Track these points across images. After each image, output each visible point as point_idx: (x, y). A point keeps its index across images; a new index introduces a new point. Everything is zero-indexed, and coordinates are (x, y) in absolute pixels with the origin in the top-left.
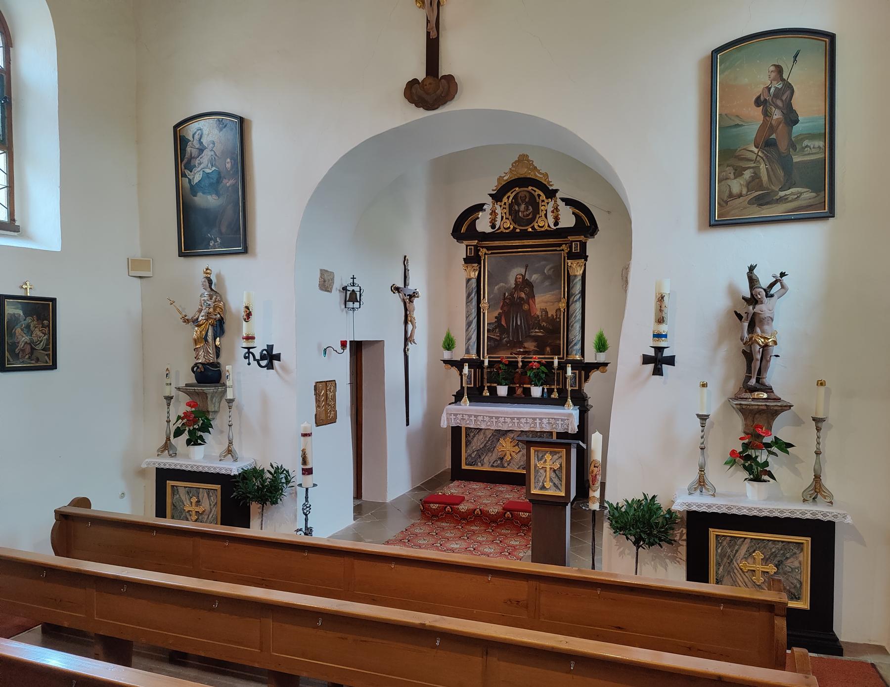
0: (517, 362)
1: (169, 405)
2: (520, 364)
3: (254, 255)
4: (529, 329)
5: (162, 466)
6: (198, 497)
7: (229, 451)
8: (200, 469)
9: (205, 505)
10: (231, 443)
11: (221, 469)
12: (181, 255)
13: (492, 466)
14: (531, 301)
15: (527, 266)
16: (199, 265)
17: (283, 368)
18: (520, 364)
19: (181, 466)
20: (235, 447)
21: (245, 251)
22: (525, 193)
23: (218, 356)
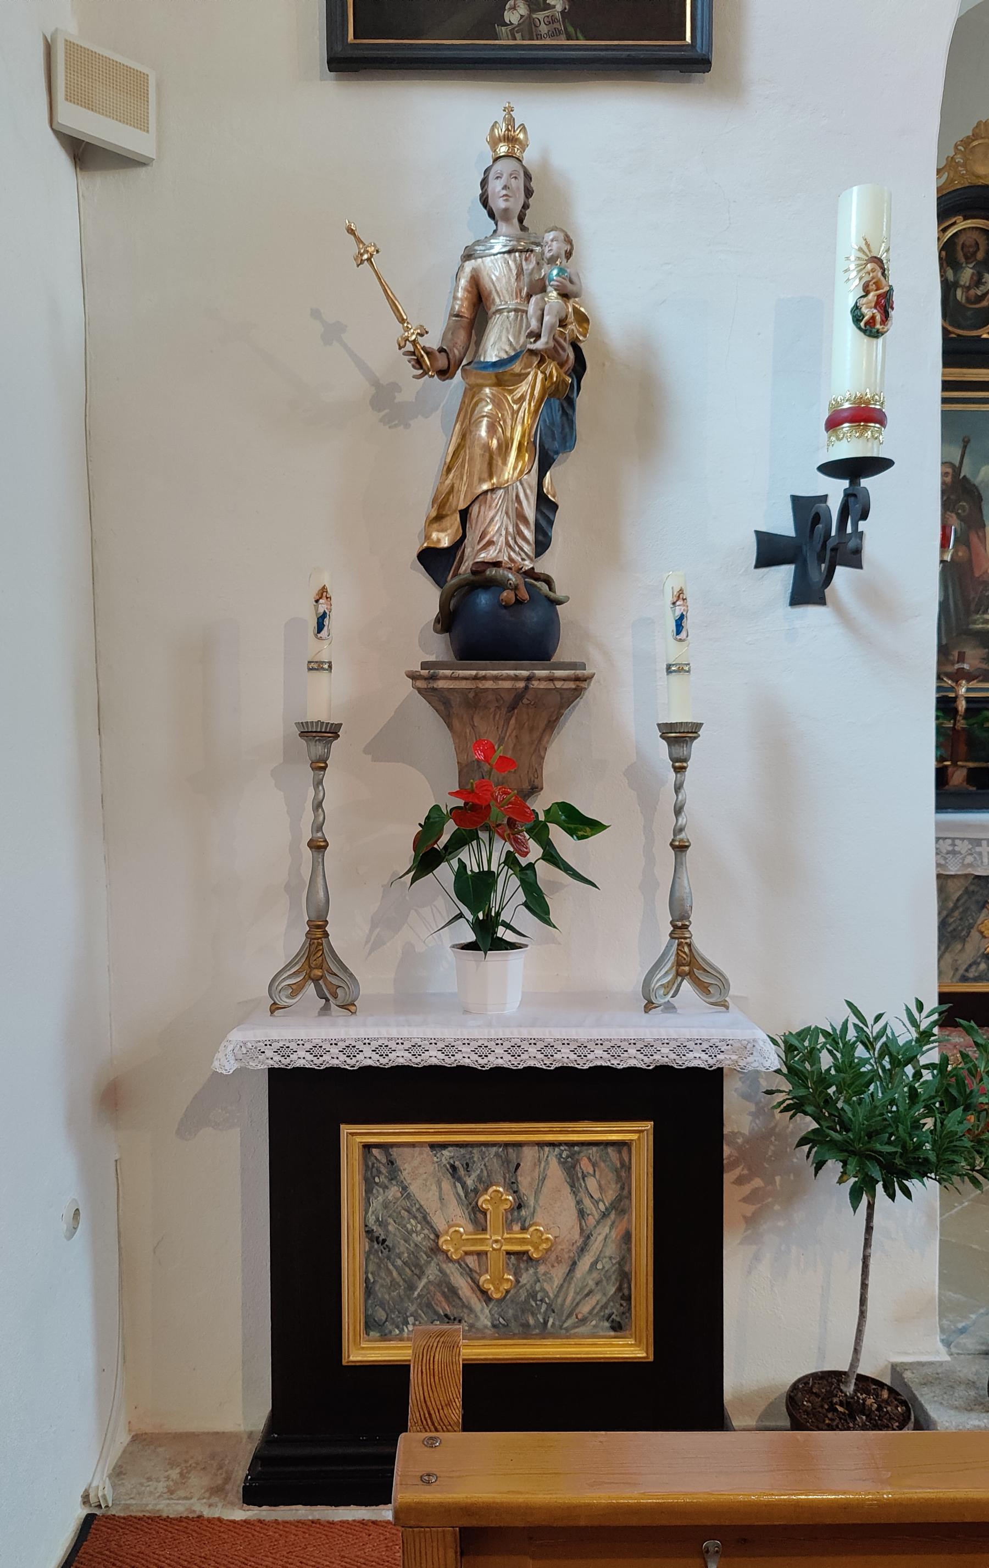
0: (955, 700)
1: (320, 765)
2: (962, 705)
3: (734, 89)
4: (968, 613)
5: (301, 1059)
6: (513, 1187)
7: (688, 965)
8: (565, 1057)
9: (555, 1217)
10: (680, 927)
11: (682, 1047)
12: (344, 62)
13: (964, 979)
14: (974, 539)
15: (966, 443)
16: (446, 127)
17: (876, 598)
18: (962, 705)
19: (449, 1048)
20: (703, 939)
21: (693, 64)
22: (975, 235)
23: (542, 544)
